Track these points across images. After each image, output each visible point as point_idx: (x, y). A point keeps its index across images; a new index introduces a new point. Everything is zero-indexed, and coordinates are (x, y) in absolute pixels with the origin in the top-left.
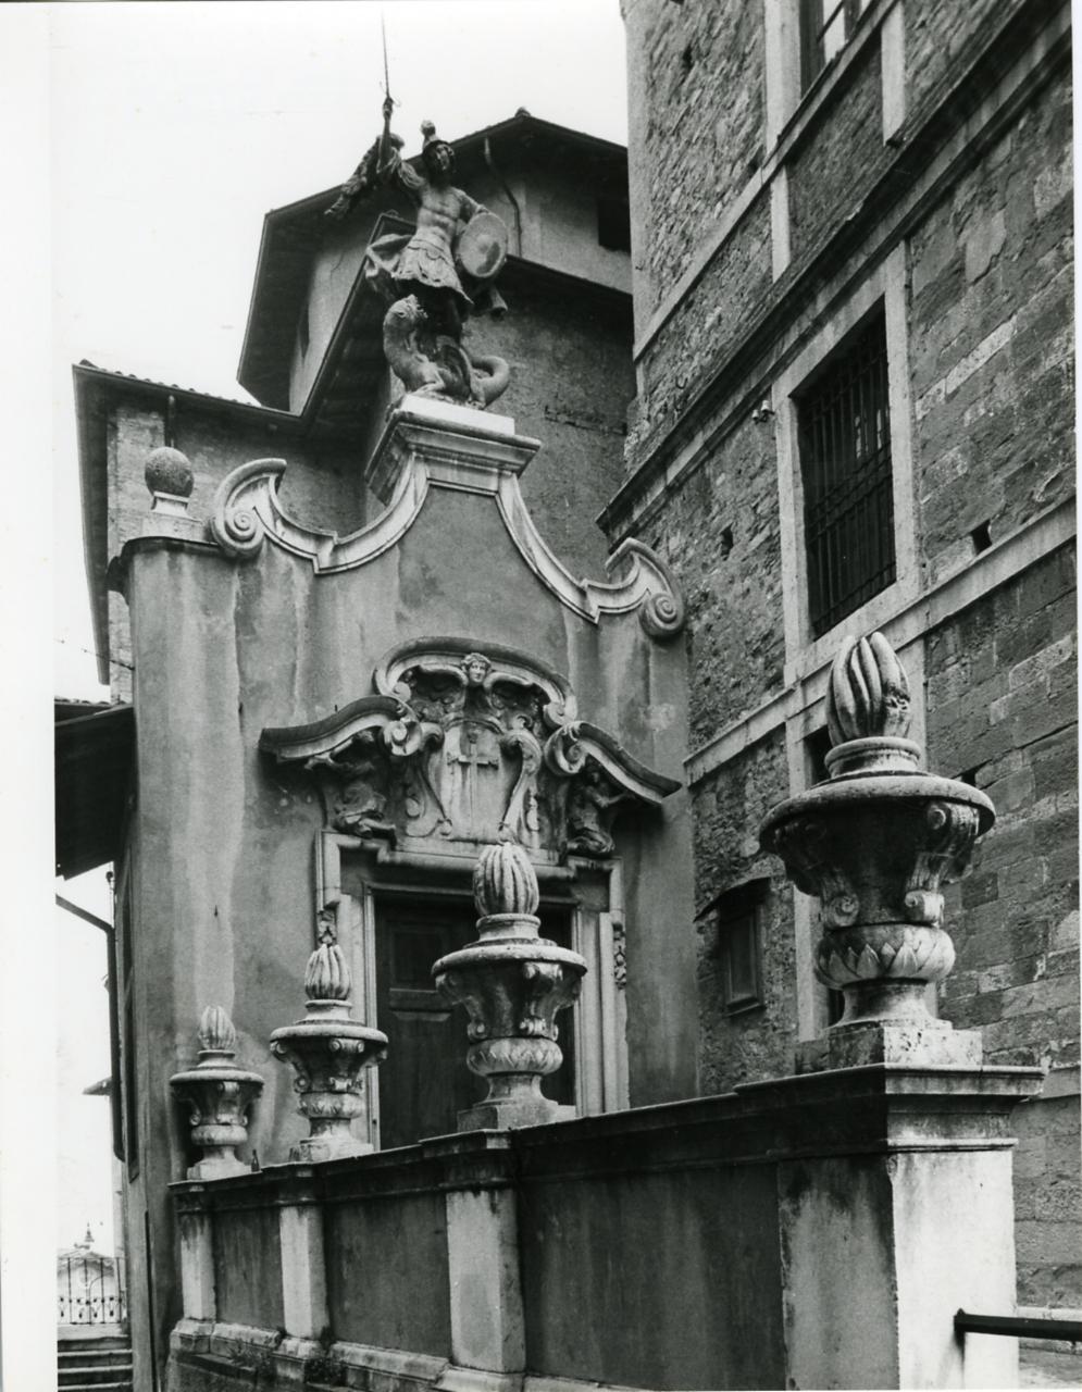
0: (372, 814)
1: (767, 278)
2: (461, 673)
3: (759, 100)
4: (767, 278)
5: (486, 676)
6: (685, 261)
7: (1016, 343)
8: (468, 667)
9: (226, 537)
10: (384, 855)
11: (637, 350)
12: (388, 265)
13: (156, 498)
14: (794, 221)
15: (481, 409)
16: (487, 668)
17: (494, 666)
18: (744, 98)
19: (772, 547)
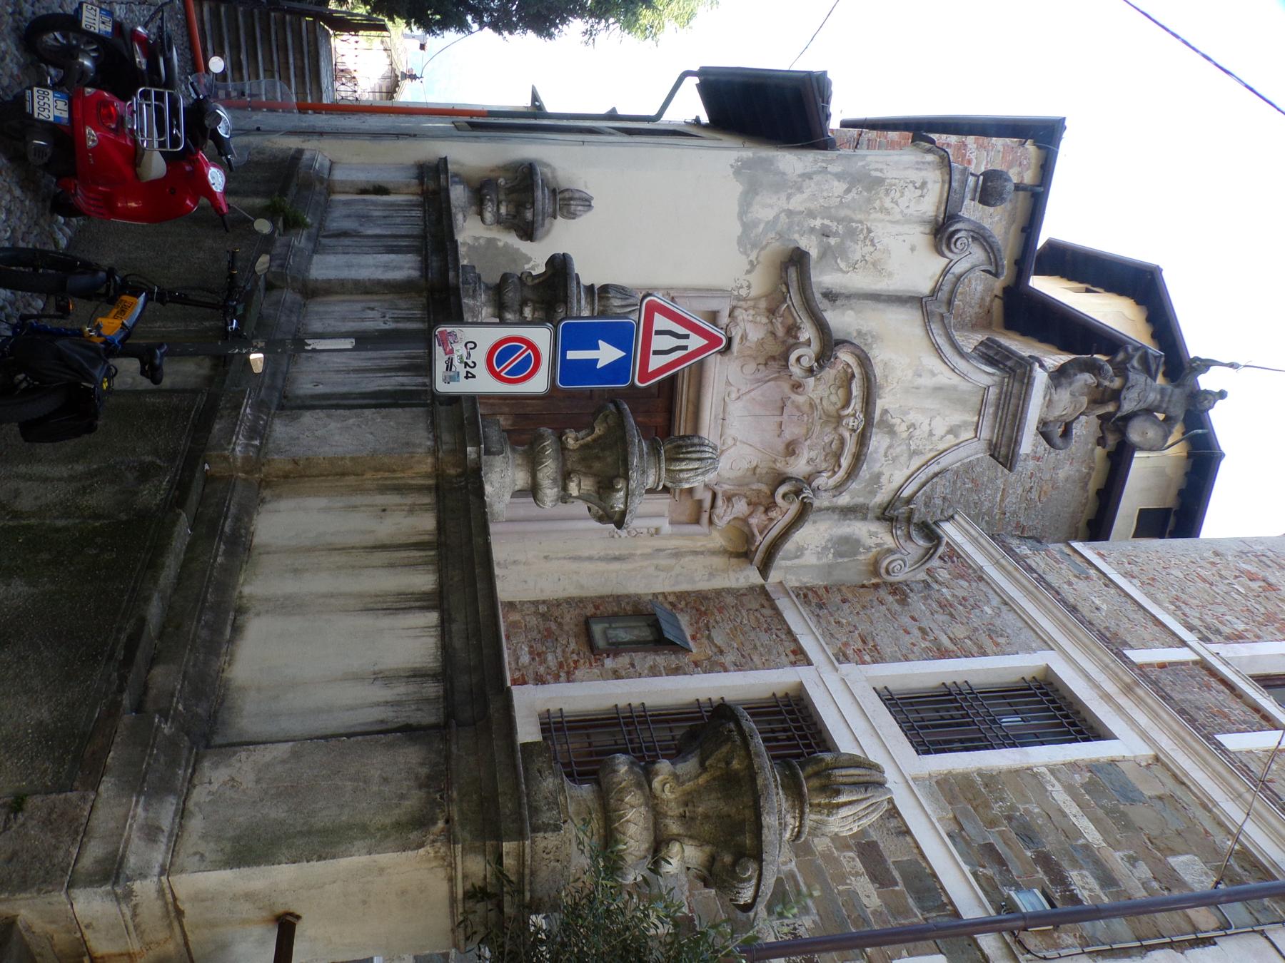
0: (744, 337)
1: (1125, 644)
2: (850, 411)
3: (1239, 637)
4: (1125, 644)
6: (1136, 581)
7: (1087, 847)
8: (854, 415)
9: (952, 229)
11: (1077, 545)
12: (1135, 363)
13: (978, 177)
14: (1163, 666)
15: (1037, 428)
16: (854, 431)
17: (855, 436)
18: (1241, 627)
19: (943, 654)
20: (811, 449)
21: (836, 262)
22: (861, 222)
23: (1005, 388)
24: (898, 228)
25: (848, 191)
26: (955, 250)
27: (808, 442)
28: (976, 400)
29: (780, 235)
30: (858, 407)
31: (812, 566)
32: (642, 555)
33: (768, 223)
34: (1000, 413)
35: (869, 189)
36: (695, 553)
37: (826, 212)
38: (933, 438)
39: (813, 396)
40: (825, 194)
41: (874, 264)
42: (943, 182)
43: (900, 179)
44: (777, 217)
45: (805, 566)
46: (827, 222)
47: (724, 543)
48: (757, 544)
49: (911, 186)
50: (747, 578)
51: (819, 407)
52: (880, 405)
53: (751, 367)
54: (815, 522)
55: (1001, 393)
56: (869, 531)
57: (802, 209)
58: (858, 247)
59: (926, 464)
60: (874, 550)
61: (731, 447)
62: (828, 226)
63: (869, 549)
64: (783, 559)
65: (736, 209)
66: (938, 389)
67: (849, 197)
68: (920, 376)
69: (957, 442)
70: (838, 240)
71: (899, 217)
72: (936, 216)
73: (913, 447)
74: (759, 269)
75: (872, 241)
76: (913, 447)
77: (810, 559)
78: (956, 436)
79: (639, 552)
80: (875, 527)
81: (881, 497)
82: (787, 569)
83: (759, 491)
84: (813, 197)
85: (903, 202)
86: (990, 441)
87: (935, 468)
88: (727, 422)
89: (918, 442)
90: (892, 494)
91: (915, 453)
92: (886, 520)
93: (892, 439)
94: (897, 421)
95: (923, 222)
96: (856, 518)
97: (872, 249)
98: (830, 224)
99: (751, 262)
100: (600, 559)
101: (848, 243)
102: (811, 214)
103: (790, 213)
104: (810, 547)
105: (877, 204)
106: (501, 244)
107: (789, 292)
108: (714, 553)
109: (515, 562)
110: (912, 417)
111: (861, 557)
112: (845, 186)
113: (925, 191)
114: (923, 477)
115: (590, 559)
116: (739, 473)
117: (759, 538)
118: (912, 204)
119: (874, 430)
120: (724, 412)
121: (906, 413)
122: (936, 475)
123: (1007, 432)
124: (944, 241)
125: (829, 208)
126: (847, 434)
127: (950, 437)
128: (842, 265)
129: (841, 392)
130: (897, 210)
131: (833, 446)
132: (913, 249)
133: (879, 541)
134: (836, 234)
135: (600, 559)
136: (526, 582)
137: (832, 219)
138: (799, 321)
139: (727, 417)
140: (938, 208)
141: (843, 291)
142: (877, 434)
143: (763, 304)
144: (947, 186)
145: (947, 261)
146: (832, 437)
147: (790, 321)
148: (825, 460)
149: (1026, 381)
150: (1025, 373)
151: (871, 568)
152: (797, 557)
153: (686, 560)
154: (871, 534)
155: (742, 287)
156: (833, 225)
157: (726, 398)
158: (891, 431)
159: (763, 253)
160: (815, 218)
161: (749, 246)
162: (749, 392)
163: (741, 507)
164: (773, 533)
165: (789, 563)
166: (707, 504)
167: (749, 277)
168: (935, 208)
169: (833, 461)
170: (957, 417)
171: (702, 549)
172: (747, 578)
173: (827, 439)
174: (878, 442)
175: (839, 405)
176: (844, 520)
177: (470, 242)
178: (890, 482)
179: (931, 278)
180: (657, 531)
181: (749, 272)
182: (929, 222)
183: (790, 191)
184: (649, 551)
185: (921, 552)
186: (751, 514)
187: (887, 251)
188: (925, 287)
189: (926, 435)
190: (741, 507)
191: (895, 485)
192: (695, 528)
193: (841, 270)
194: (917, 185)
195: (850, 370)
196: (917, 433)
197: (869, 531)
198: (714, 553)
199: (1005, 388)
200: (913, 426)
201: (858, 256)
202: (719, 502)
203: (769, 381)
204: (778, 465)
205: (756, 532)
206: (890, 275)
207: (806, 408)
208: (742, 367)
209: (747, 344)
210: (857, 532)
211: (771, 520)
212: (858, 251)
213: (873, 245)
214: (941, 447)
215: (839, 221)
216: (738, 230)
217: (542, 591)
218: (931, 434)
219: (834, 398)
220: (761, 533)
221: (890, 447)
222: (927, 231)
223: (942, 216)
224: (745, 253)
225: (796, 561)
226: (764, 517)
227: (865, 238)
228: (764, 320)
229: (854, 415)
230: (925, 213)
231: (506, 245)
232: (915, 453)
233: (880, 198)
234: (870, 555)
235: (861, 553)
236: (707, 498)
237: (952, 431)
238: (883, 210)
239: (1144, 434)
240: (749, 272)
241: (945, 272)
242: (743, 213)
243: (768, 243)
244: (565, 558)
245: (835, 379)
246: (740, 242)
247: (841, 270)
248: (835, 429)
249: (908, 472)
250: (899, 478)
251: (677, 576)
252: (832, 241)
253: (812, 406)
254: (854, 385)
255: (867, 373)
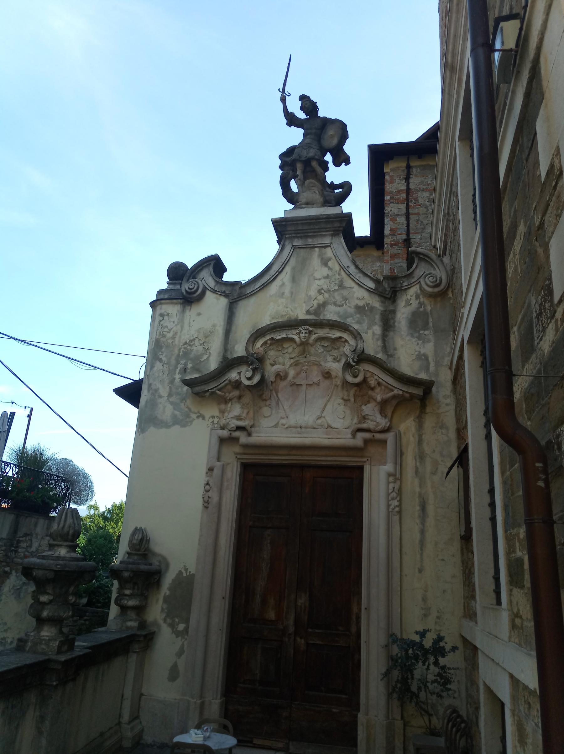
0: (239, 418)
2: (296, 338)
5: (309, 337)
8: (299, 334)
10: (244, 439)
16: (310, 332)
17: (316, 331)
20: (326, 361)
21: (203, 362)
22: (180, 349)
23: (293, 235)
24: (186, 327)
25: (160, 360)
26: (195, 288)
27: (322, 363)
28: (302, 252)
29: (183, 400)
30: (294, 332)
31: (435, 346)
32: (420, 486)
33: (174, 409)
34: (311, 234)
35: (161, 347)
36: (420, 442)
37: (171, 373)
38: (330, 275)
39: (288, 364)
40: (161, 374)
41: (206, 337)
42: (161, 304)
43: (157, 330)
44: (172, 403)
45: (436, 351)
46: (177, 371)
47: (412, 419)
48: (401, 393)
49: (161, 323)
50: (445, 397)
51: (297, 359)
52: (302, 316)
53: (266, 411)
54: (395, 349)
55: (297, 237)
56: (405, 306)
57: (168, 388)
58: (195, 349)
59: (349, 275)
60: (422, 300)
61: (326, 420)
62: (180, 370)
63: (421, 304)
64: (427, 368)
65: (164, 430)
66: (294, 280)
67: (164, 359)
68: (283, 294)
69: (334, 258)
70: (189, 362)
71: (179, 327)
72: (181, 304)
73: (336, 288)
74: (202, 412)
75: (191, 341)
76: (336, 288)
77: (429, 349)
78: (330, 259)
79: (418, 490)
80: (401, 303)
81: (376, 303)
82: (438, 364)
83: (355, 395)
84: (162, 382)
85: (170, 325)
86: (332, 235)
87: (352, 269)
88: (303, 425)
89: (332, 285)
90: (373, 295)
91: (341, 286)
92: (395, 295)
93: (329, 304)
94: (315, 303)
95: (184, 311)
96: (393, 318)
97: (197, 340)
98: (179, 368)
99: (198, 417)
100: (423, 522)
101: (192, 356)
102: (172, 382)
103: (170, 395)
104: (418, 349)
105: (170, 341)
106: (168, 593)
107: (208, 391)
108: (420, 426)
109: (424, 600)
110: (313, 293)
111: (429, 308)
112: (158, 363)
113: (165, 313)
114: (359, 276)
115: (422, 532)
116: (348, 412)
117: (396, 392)
118: (172, 320)
119: (322, 317)
120: (296, 427)
121: (310, 297)
122: (357, 267)
123: (323, 225)
124: (191, 296)
125: (169, 370)
126: (314, 337)
127: (330, 264)
128: (205, 357)
129: (286, 345)
130: (175, 329)
131: (326, 345)
132: (199, 314)
133: (414, 297)
134: (186, 364)
135: (423, 522)
136: (444, 591)
137: (176, 367)
138: (227, 382)
139: (299, 425)
140: (176, 304)
141: (222, 354)
142: (324, 315)
143: (223, 406)
144: (163, 301)
145: (208, 293)
146: (319, 347)
147: (229, 387)
148: (338, 349)
149: (284, 223)
150: (279, 225)
151: (439, 299)
152: (427, 359)
153: (426, 448)
154: (408, 303)
155: (213, 422)
156: (180, 366)
157: (285, 427)
158: (323, 305)
159: (193, 410)
160: (175, 379)
161: (188, 420)
162: (284, 410)
163: (369, 409)
164: (390, 380)
165: (432, 365)
166: (367, 435)
167: (207, 418)
168: (176, 306)
169: (338, 344)
170: (315, 261)
171: (417, 436)
172: (445, 397)
173: (321, 350)
174: (331, 314)
175: (294, 345)
176: (394, 326)
177: (164, 615)
178: (363, 298)
179: (218, 299)
180: (389, 475)
181: (204, 418)
182: (184, 307)
183: (157, 397)
184: (417, 481)
185: (423, 264)
186: (375, 400)
187: (198, 331)
188: (223, 302)
189: (327, 281)
190: (369, 409)
191: (365, 294)
192: (389, 443)
193: (208, 358)
194: (161, 318)
195: (269, 342)
196: (325, 287)
197: (405, 306)
198: (420, 426)
199: (293, 235)
200: (320, 292)
201: (201, 348)
202: (365, 426)
203: (278, 396)
204: (338, 383)
205: (391, 394)
206: (214, 326)
207: (298, 368)
208: (265, 417)
209: (244, 415)
210: (405, 316)
211: (379, 384)
212: (198, 349)
213: (194, 340)
214: (337, 268)
215: (178, 363)
216: (177, 428)
217: (454, 576)
218: (327, 277)
219: (290, 350)
220: (392, 391)
221: (335, 304)
222: (189, 307)
223: (179, 300)
224: (191, 422)
225: (430, 359)
226: (378, 390)
227: (190, 345)
228: (230, 405)
229: (299, 334)
230: (178, 311)
231: (169, 589)
232: (341, 286)
233: (167, 340)
234: (426, 302)
235: (425, 309)
236: (360, 435)
237: (325, 263)
238: (173, 338)
239: (332, 136)
240: (204, 418)
241: (214, 291)
242: (167, 425)
243: (187, 407)
244: (421, 554)
245: (278, 351)
246: (184, 426)
247: (208, 358)
248: (312, 345)
249: (356, 287)
250: (359, 293)
251: (442, 455)
252: (190, 366)
253: (296, 364)
254: (278, 338)
255: (268, 330)
